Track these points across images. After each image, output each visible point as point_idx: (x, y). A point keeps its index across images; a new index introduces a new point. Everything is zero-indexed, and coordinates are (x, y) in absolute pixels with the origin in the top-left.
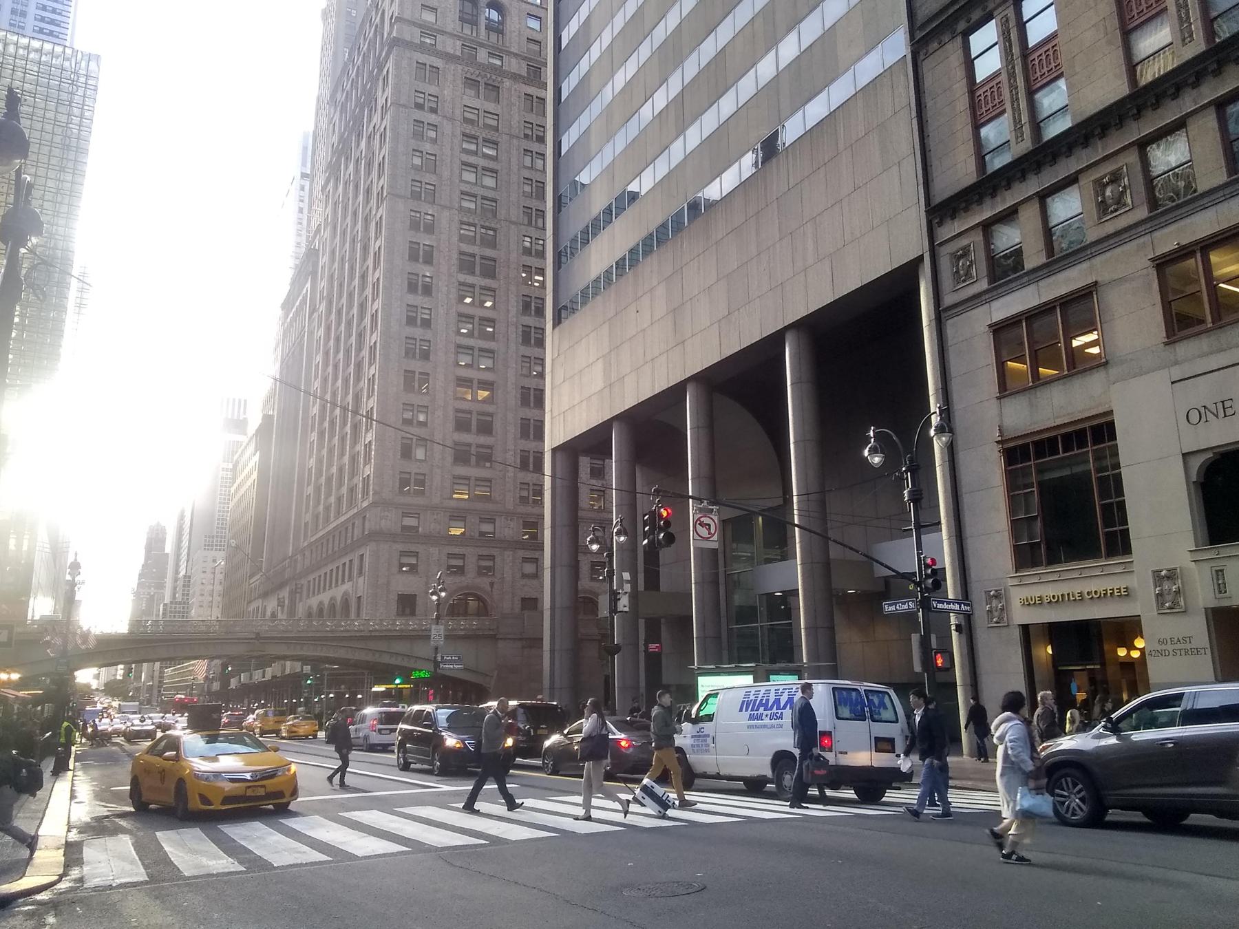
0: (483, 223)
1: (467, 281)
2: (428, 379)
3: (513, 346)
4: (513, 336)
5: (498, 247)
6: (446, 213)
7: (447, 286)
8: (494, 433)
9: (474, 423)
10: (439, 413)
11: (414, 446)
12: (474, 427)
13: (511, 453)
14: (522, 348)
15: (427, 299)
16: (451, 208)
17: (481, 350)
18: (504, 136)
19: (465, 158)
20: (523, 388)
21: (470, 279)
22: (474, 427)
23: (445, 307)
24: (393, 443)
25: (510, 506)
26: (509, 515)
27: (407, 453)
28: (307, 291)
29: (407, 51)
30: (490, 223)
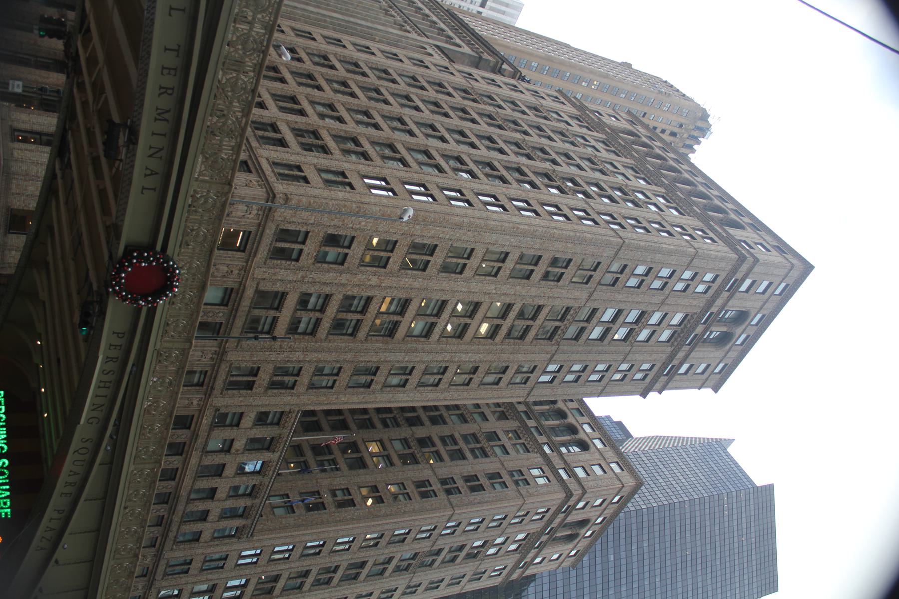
0: (562, 328)
1: (512, 312)
2: (418, 269)
3: (429, 358)
4: (439, 358)
5: (535, 342)
6: (585, 295)
7: (515, 294)
8: (331, 337)
9: (350, 316)
10: (374, 280)
11: (340, 250)
12: (343, 316)
13: (301, 358)
14: (423, 367)
15: (508, 272)
16: (588, 300)
17: (433, 325)
18: (629, 348)
19: (625, 313)
20: (377, 368)
21: (512, 315)
22: (343, 316)
23: (494, 291)
24: (351, 226)
25: (232, 356)
26: (220, 356)
27: (332, 240)
28: (459, 46)
29: (730, 267)
30: (560, 335)
